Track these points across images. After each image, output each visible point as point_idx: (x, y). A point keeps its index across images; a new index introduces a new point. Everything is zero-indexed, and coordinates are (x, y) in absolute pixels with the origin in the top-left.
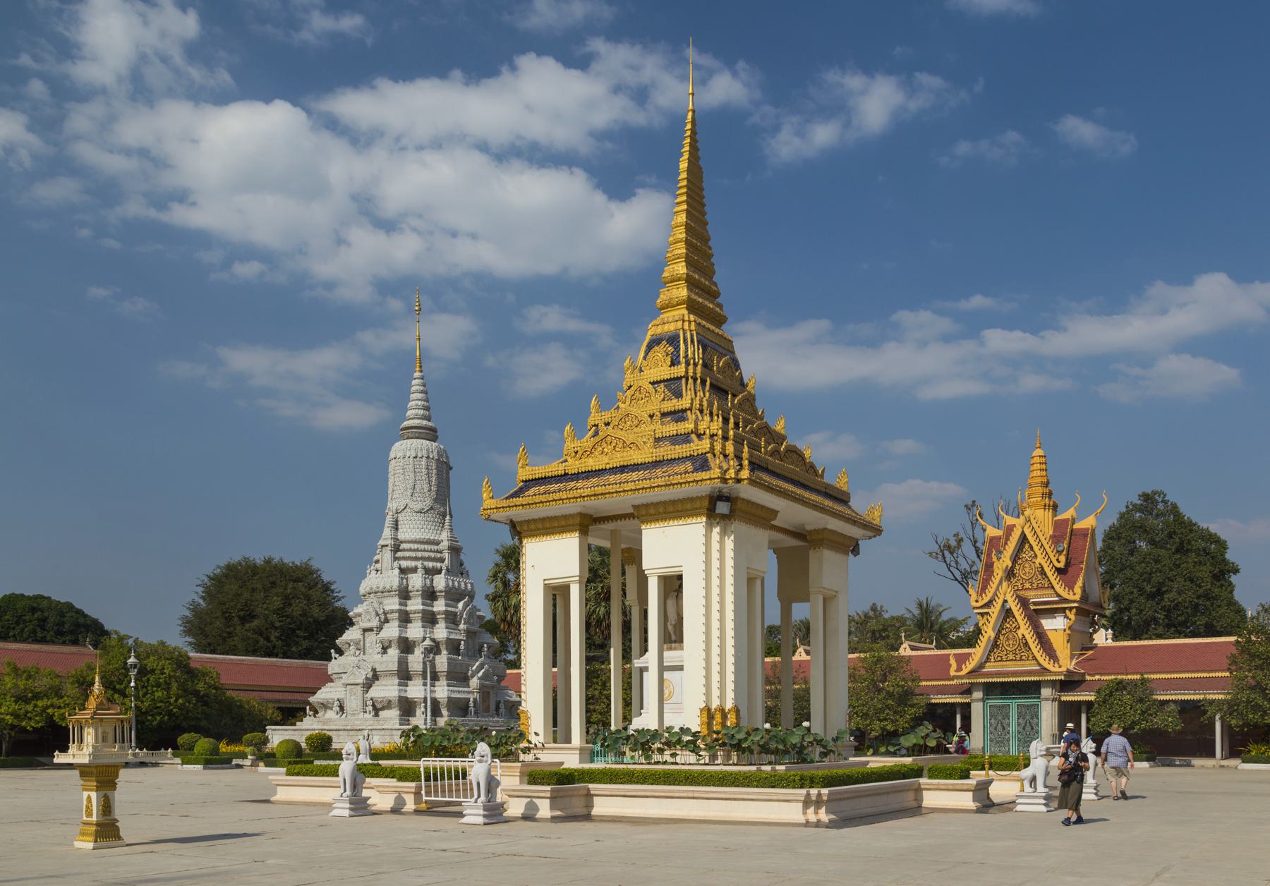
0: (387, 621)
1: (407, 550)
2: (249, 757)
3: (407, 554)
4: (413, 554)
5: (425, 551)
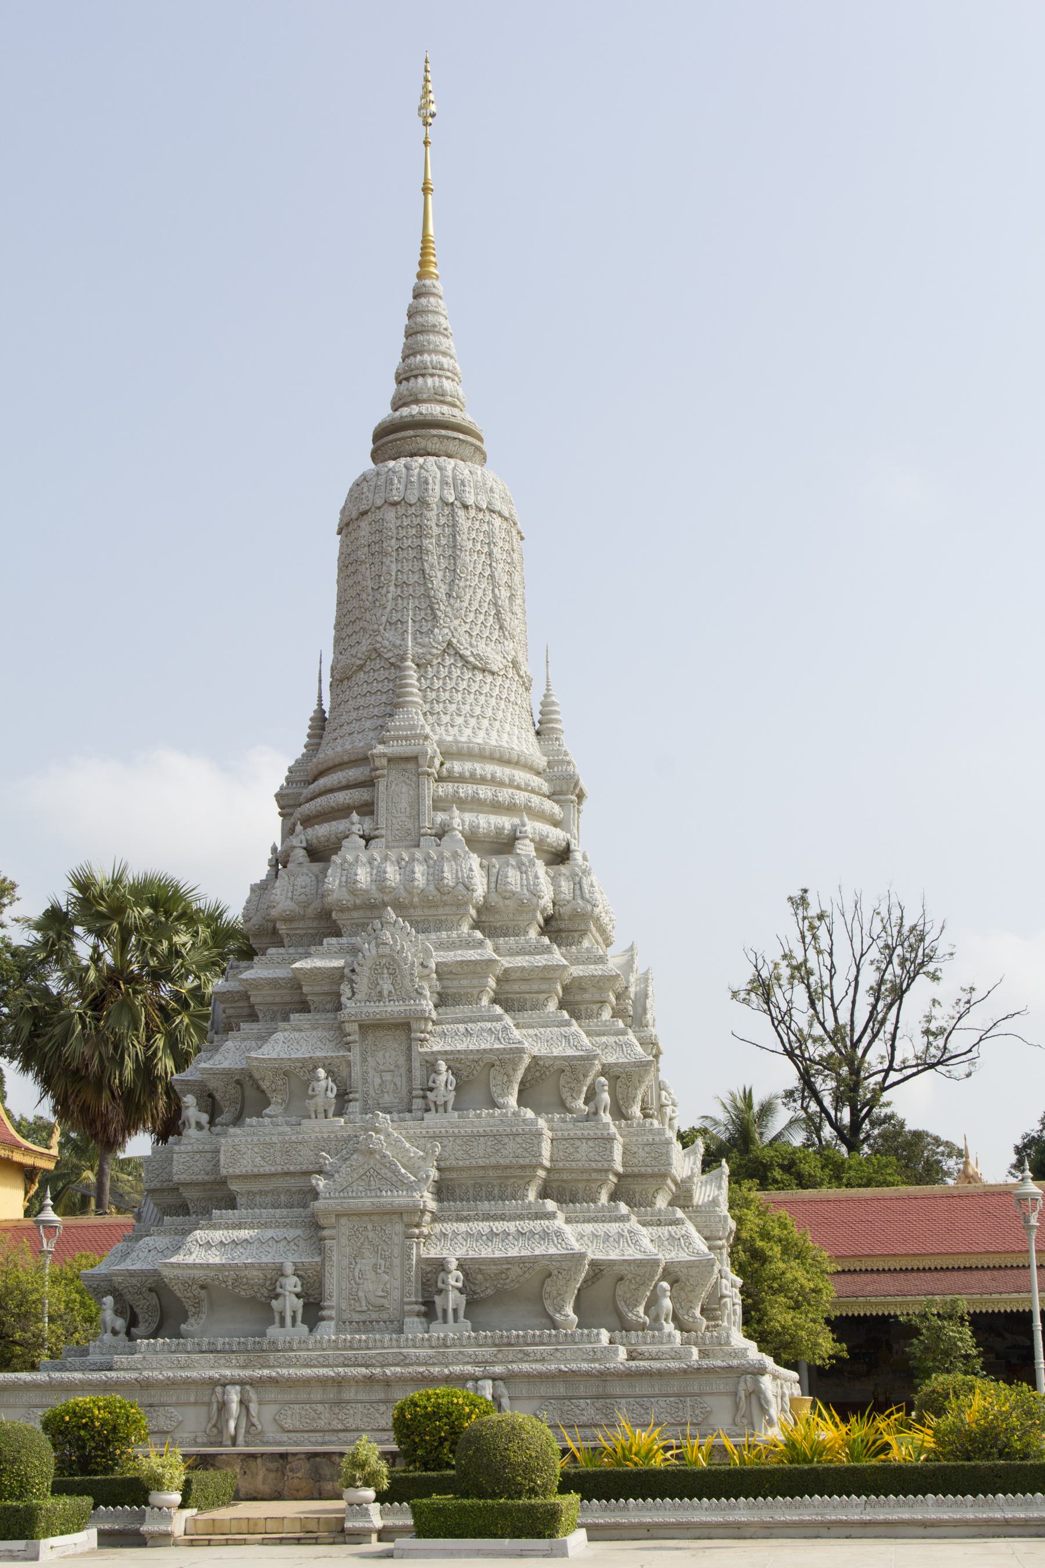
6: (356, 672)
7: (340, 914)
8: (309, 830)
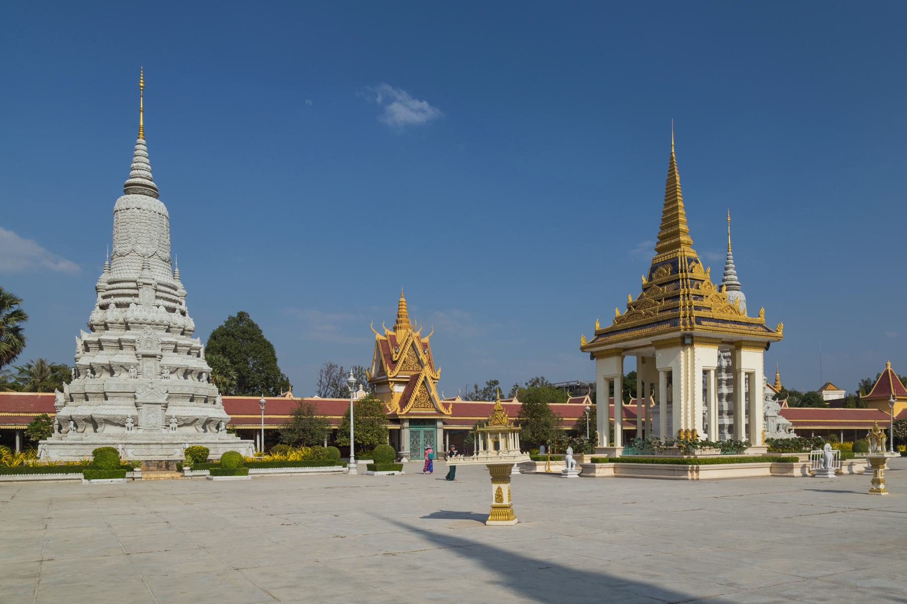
1: (162, 291)
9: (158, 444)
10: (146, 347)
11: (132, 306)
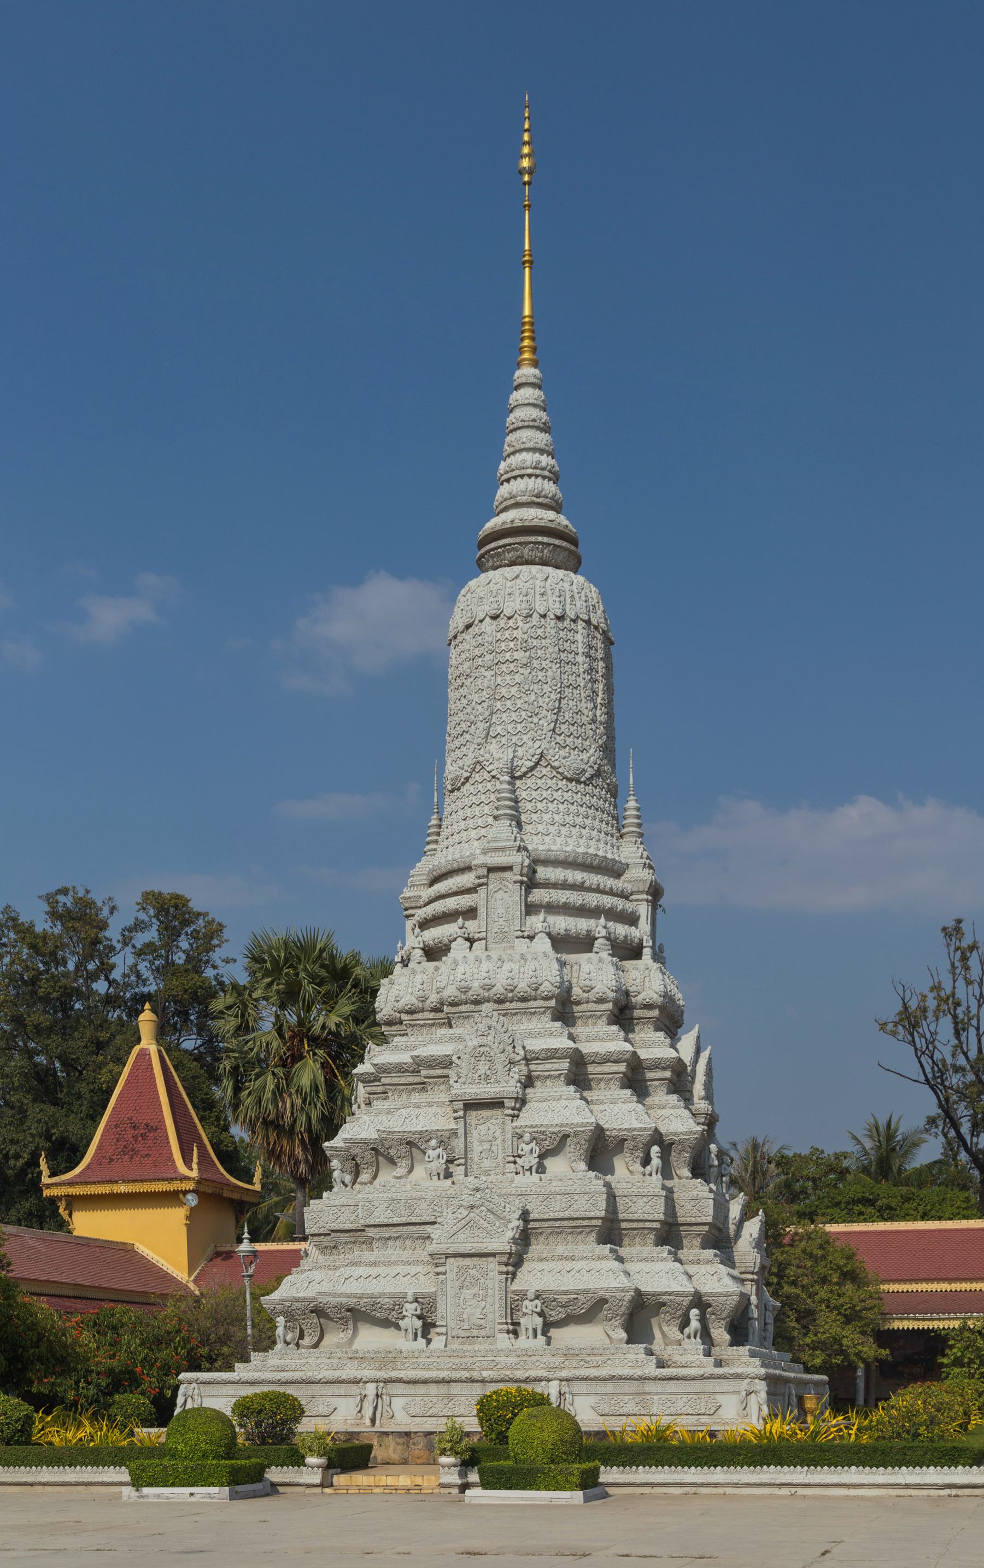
0: (529, 1082)
2: (311, 1460)
3: (562, 896)
4: (575, 898)
5: (598, 890)
6: (463, 784)
7: (450, 1007)
8: (426, 933)
9: (472, 1381)
10: (476, 1076)
11: (459, 949)
